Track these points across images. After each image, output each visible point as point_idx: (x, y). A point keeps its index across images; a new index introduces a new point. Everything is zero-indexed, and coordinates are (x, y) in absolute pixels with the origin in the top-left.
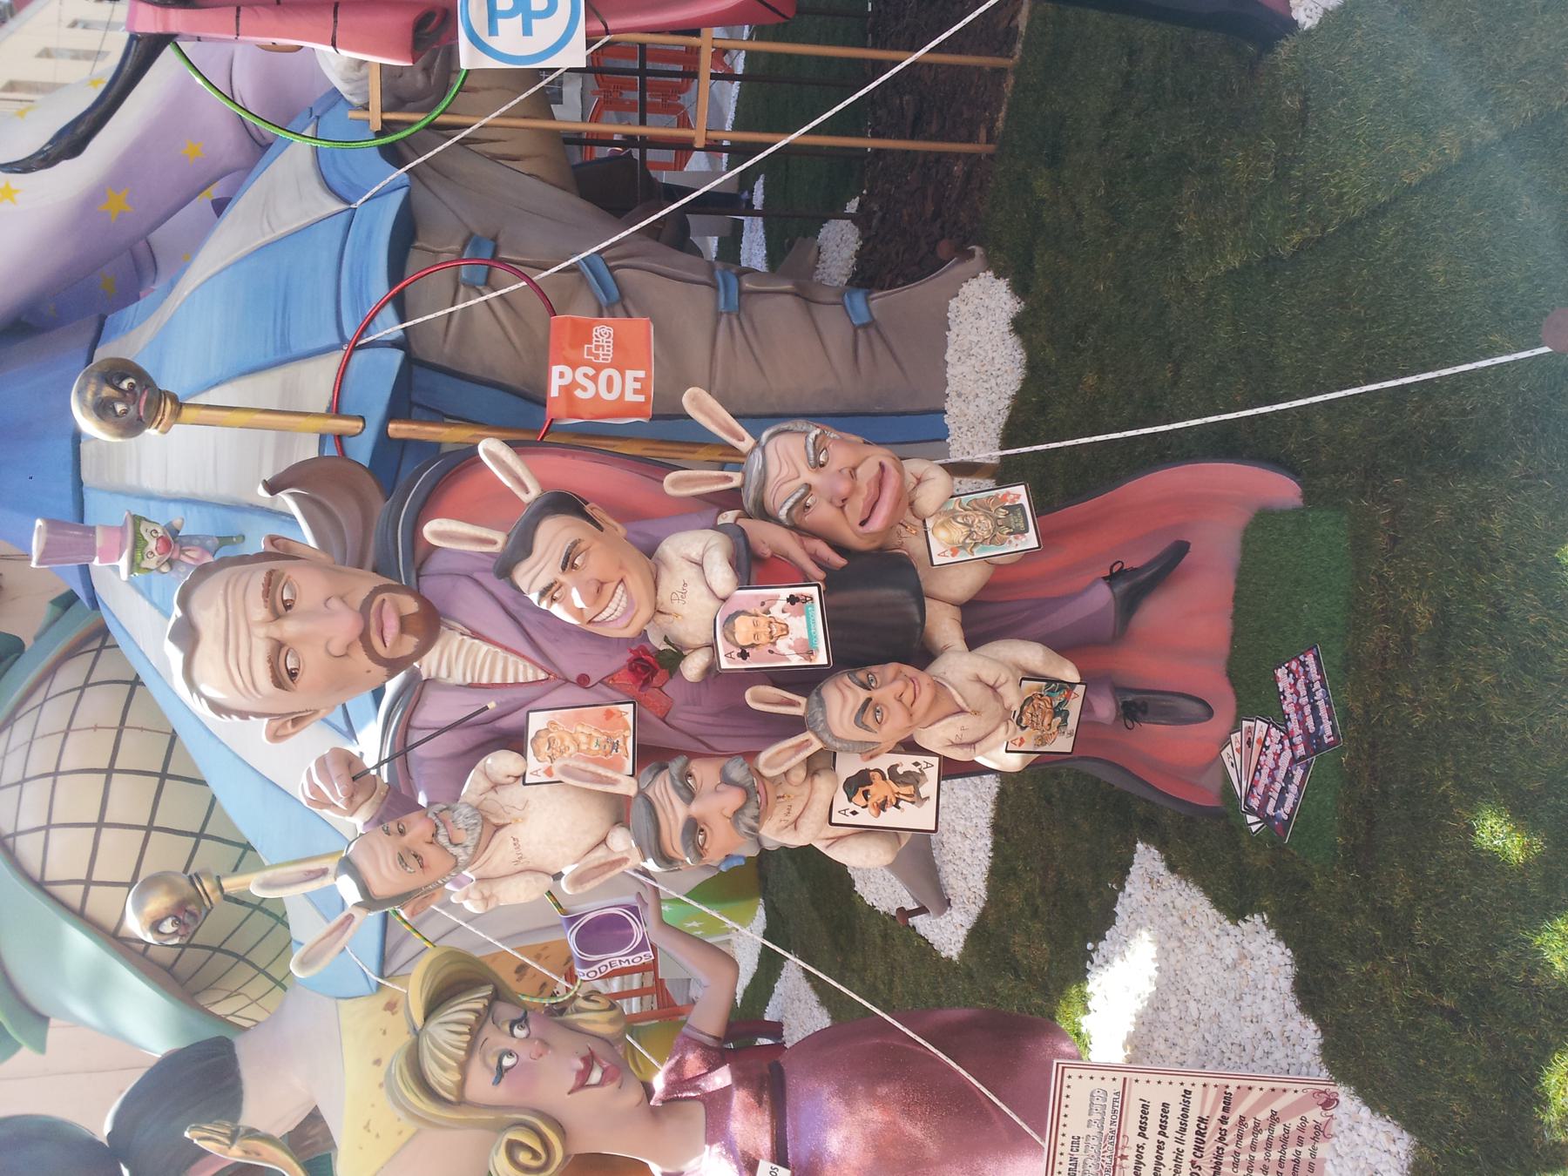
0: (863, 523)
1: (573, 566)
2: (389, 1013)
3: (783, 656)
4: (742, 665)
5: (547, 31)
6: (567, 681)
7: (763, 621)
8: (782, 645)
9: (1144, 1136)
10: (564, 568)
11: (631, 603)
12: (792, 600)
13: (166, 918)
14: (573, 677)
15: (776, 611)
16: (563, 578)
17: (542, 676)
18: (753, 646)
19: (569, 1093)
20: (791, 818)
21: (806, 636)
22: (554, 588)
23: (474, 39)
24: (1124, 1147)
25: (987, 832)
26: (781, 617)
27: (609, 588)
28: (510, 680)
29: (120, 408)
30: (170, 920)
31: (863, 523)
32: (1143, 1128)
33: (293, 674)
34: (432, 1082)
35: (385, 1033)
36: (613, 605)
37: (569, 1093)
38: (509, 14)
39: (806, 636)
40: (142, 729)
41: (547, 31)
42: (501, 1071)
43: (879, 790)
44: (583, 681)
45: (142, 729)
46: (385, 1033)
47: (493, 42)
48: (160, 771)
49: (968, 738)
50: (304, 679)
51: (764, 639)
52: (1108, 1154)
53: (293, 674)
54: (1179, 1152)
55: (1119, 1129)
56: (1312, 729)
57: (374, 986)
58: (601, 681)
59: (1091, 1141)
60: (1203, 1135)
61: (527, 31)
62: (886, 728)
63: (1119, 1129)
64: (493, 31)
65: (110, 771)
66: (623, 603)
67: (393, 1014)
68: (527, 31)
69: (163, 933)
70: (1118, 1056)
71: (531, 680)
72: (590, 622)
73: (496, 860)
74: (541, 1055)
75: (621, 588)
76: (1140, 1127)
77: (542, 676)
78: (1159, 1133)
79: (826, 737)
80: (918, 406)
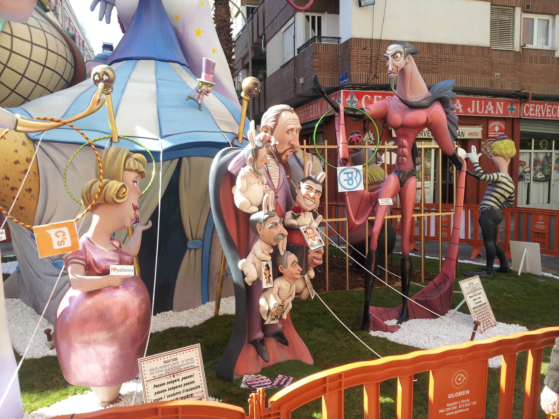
0: (313, 257)
1: (316, 192)
2: (22, 143)
3: (309, 240)
4: (303, 232)
5: (345, 184)
6: (276, 194)
7: (313, 235)
8: (311, 240)
9: (182, 380)
10: (316, 191)
11: (311, 206)
12: (320, 240)
13: (109, 77)
14: (277, 195)
15: (316, 237)
16: (314, 191)
17: (276, 188)
18: (308, 233)
19: (133, 204)
20: (264, 251)
21: (315, 245)
22: (312, 189)
23: (343, 170)
24: (177, 375)
25: (155, 331)
26: (316, 239)
27: (313, 200)
28: (272, 180)
29: (256, 88)
30: (108, 78)
31: (313, 257)
32: (185, 378)
33: (288, 133)
34: (128, 161)
35: (15, 141)
36: (310, 202)
37: (133, 204)
38: (348, 177)
39: (315, 245)
40: (57, 61)
41: (345, 184)
42: (134, 182)
43: (267, 272)
44: (276, 197)
45: (57, 61)
46: (15, 141)
47: (342, 174)
48: (46, 65)
49: (280, 292)
50: (287, 135)
51: (310, 236)
52: (174, 371)
53: (288, 133)
54: (180, 393)
55: (183, 371)
56: (282, 384)
57: (37, 138)
58: (277, 202)
59: (177, 364)
60: (187, 397)
61: (345, 180)
62: (292, 268)
63: (183, 371)
64: (345, 173)
65: (47, 49)
66: (311, 204)
67: (22, 144)
68: (345, 180)
69: (103, 75)
70: (140, 385)
71: (274, 185)
72: (304, 197)
73: (252, 178)
74: (139, 194)
75: (313, 203)
76: (157, 385)
77: (276, 188)
78: (185, 384)
79: (286, 255)
80: (210, 293)
